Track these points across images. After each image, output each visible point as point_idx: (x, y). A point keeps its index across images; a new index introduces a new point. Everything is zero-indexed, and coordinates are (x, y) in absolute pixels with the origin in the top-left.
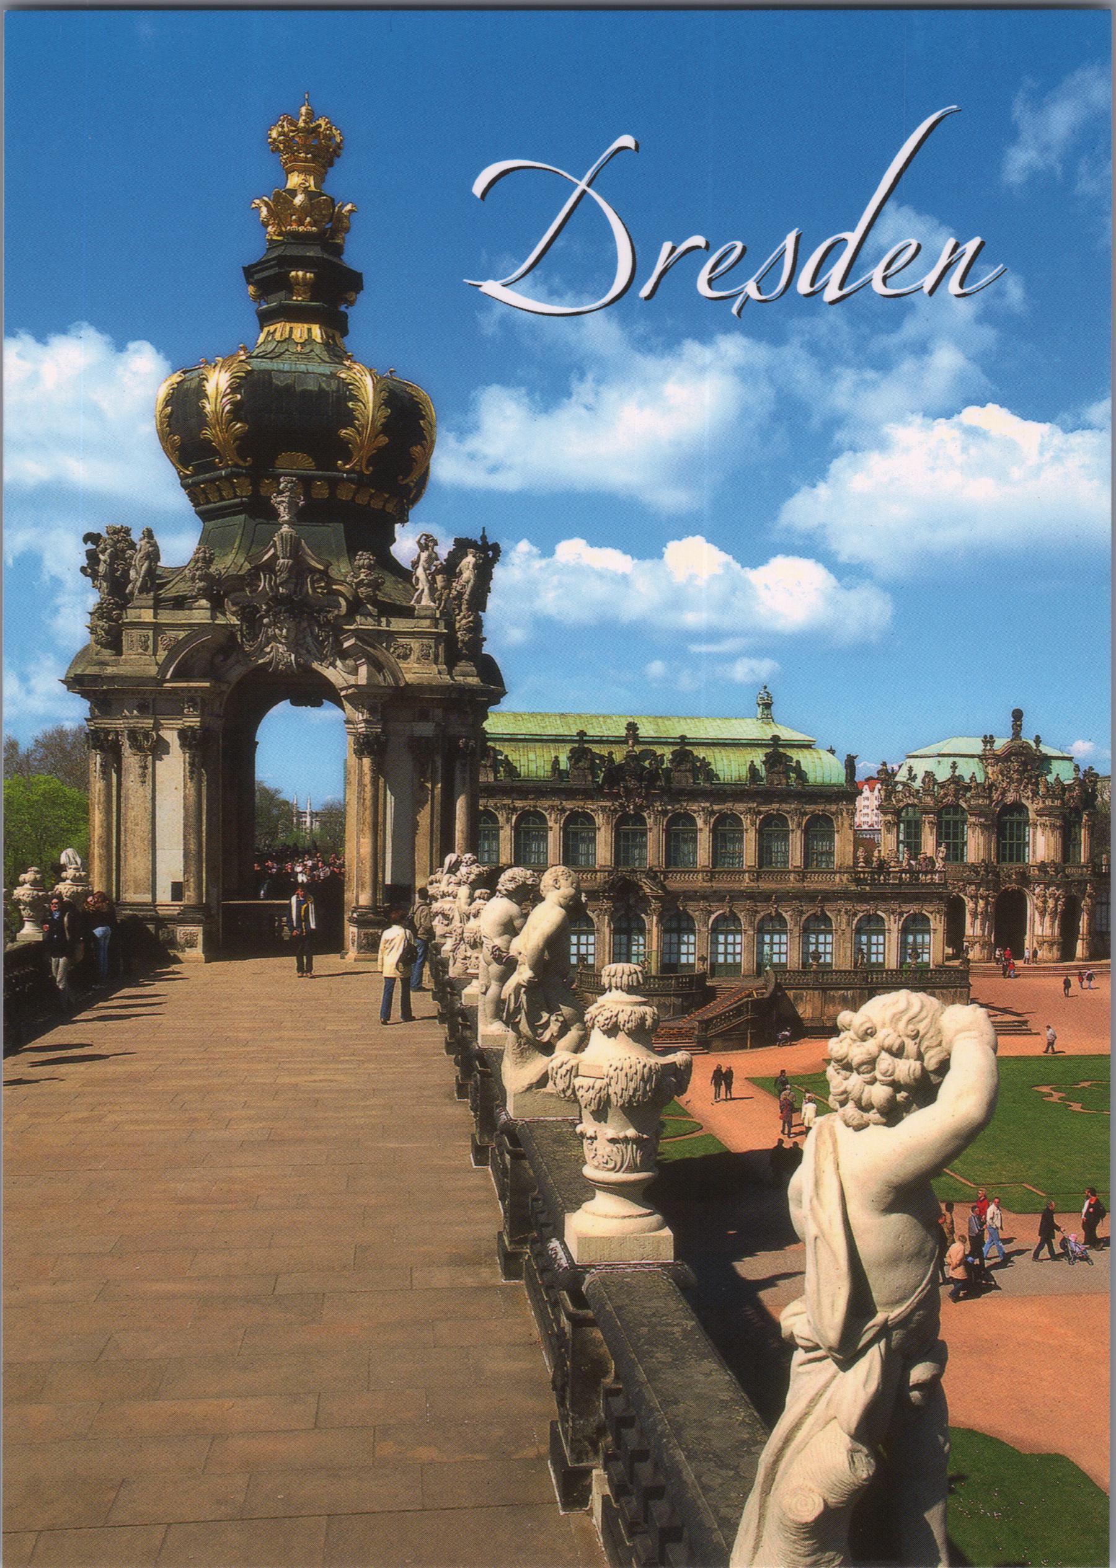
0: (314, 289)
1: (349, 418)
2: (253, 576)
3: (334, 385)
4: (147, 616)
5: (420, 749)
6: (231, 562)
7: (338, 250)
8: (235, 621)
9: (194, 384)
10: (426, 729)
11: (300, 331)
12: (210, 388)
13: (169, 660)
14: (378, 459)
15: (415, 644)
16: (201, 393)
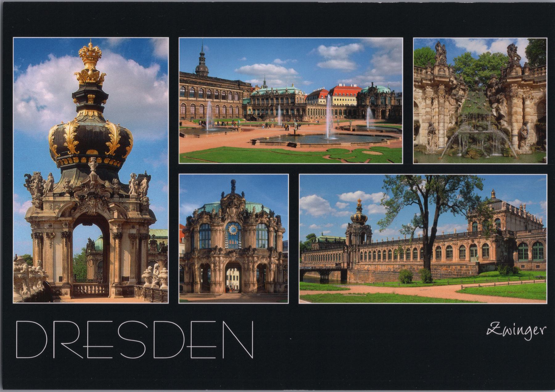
0: (95, 100)
1: (109, 139)
2: (84, 186)
3: (104, 129)
4: (51, 199)
5: (132, 237)
6: (75, 182)
7: (100, 87)
8: (77, 200)
9: (62, 129)
10: (134, 231)
11: (91, 113)
12: (67, 131)
13: (59, 211)
14: (117, 151)
15: (131, 206)
16: (64, 132)
